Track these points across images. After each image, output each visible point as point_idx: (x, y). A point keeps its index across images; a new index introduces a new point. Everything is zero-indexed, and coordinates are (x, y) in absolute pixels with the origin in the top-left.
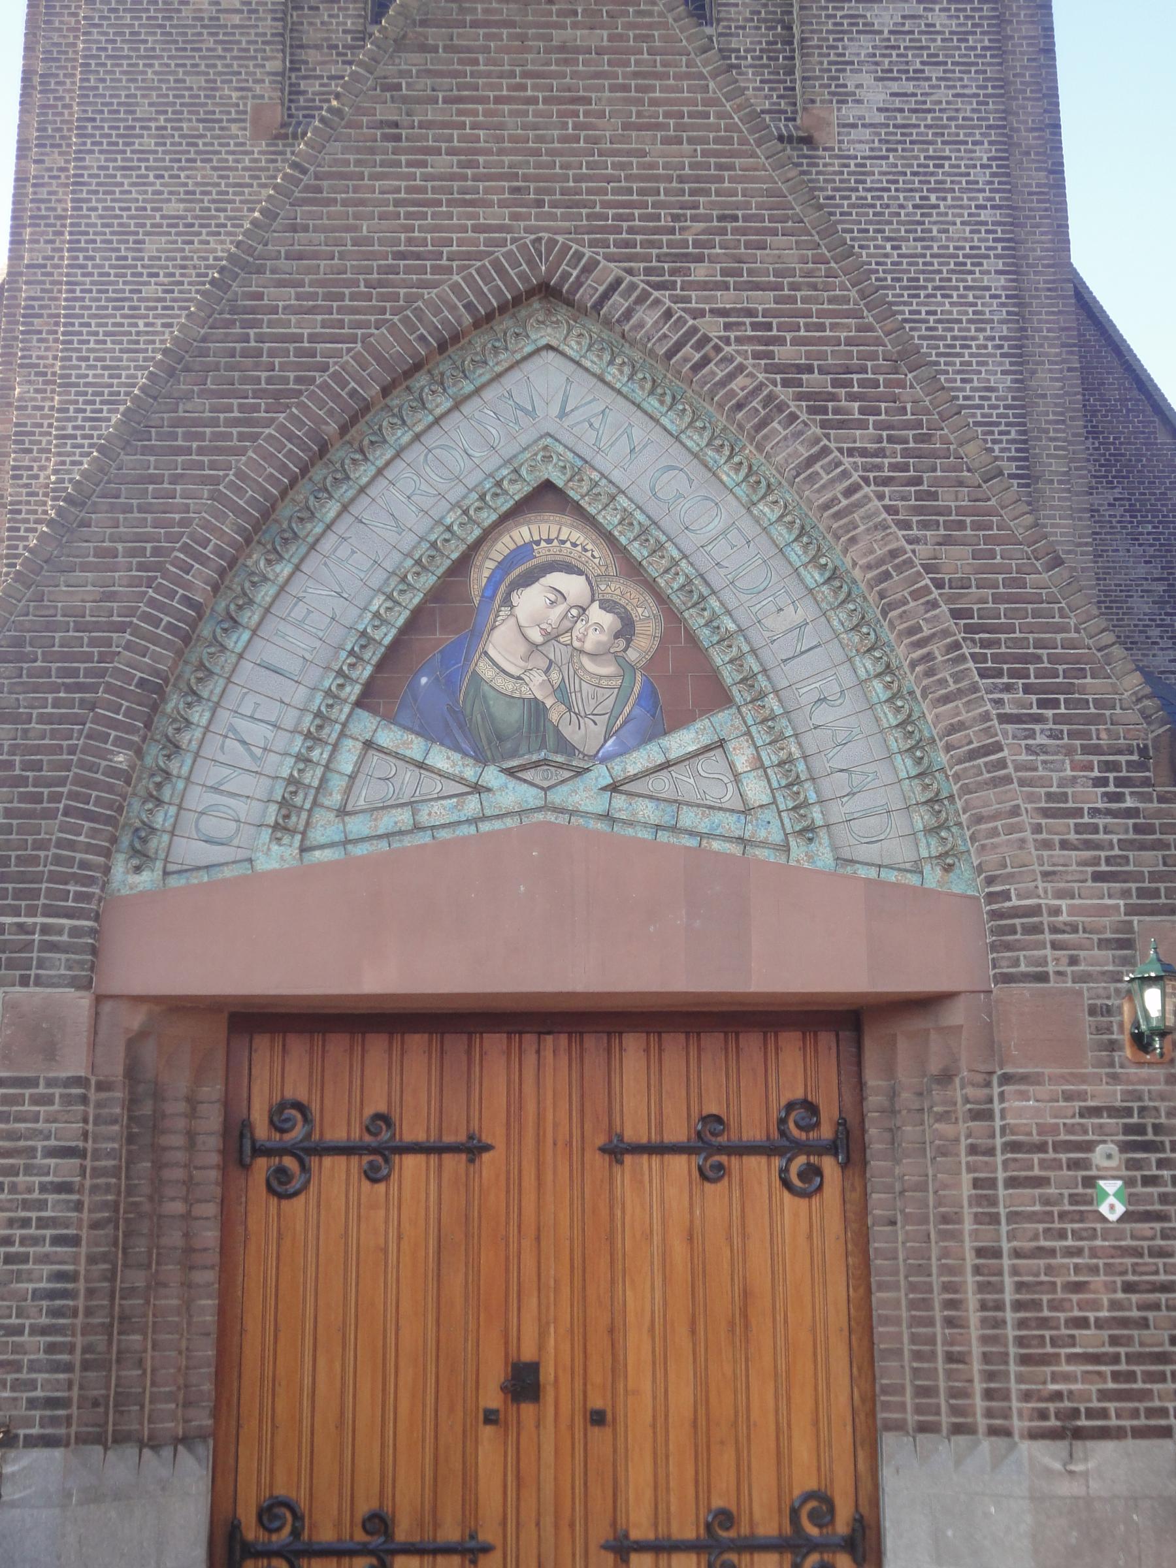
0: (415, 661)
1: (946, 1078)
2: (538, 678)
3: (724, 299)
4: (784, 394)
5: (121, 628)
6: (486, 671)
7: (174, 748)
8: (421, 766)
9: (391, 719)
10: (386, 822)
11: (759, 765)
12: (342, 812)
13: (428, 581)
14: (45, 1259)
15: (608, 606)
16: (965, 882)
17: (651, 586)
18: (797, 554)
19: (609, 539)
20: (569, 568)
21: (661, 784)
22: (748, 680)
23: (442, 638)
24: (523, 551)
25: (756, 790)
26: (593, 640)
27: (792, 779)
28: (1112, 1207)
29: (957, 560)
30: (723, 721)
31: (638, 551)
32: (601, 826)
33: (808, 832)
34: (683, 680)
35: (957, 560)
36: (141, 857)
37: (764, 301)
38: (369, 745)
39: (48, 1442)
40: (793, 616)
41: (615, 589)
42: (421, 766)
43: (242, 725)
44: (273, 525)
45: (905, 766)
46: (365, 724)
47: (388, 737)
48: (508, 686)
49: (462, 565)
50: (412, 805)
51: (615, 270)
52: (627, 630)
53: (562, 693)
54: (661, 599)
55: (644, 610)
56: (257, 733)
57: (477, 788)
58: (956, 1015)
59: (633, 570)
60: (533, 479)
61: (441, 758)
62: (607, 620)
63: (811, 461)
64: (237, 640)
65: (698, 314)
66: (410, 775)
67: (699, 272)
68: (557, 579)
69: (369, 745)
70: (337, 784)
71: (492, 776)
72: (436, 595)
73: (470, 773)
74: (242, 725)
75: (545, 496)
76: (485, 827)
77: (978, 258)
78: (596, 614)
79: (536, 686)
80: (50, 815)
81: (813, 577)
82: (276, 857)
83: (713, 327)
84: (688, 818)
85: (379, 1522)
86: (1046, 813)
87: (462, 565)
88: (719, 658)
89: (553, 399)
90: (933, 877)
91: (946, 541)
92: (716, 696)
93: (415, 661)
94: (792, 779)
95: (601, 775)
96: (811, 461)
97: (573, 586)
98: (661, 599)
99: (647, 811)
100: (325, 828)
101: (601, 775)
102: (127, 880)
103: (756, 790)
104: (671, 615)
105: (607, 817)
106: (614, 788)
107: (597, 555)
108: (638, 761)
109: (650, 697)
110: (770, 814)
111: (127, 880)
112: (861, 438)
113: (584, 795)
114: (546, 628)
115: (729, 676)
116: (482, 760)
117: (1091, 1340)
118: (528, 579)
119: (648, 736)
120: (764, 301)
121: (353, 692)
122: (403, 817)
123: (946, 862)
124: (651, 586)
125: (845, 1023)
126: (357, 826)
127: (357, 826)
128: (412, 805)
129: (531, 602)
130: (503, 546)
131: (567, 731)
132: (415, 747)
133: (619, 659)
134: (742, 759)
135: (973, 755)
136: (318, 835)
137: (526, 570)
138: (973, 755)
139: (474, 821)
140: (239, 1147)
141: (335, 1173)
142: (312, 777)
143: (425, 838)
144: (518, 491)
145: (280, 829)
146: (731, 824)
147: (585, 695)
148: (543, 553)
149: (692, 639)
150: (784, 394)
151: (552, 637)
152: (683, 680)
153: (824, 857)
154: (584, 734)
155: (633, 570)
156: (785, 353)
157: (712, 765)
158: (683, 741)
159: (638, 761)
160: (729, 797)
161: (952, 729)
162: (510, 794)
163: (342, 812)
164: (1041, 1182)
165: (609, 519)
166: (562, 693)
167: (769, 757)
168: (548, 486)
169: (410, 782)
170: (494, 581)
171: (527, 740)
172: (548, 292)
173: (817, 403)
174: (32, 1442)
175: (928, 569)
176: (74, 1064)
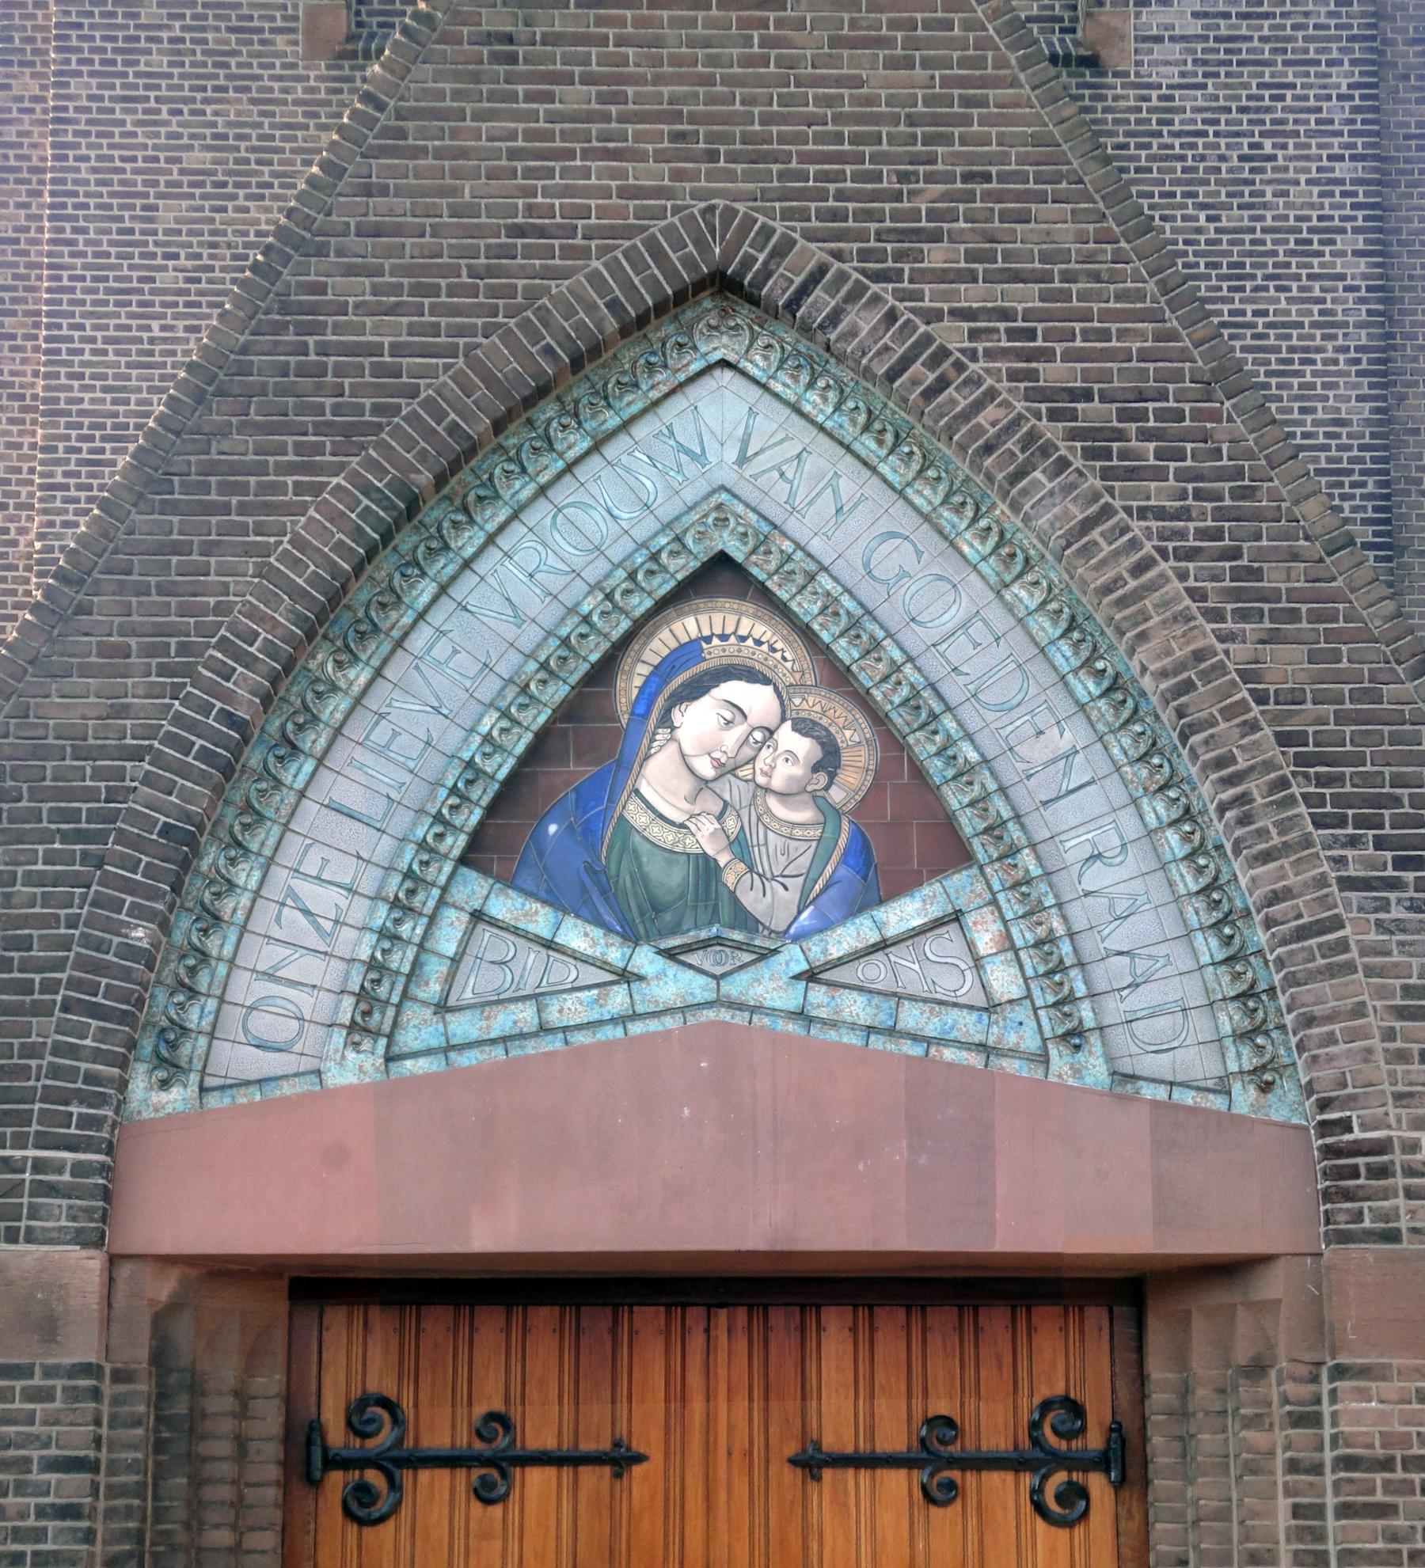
0: (541, 802)
1: (1257, 1369)
2: (706, 828)
3: (970, 296)
4: (1051, 431)
5: (137, 755)
6: (637, 816)
7: (212, 920)
8: (549, 945)
9: (508, 881)
10: (503, 1021)
11: (1008, 945)
13: (558, 692)
15: (803, 727)
16: (1287, 1107)
17: (863, 700)
18: (1064, 655)
19: (806, 634)
20: (751, 675)
21: (874, 971)
22: (994, 830)
23: (580, 771)
24: (689, 651)
25: (1004, 980)
27: (1055, 965)
29: (1287, 665)
30: (961, 885)
31: (845, 651)
32: (793, 1027)
33: (1074, 1038)
34: (907, 827)
35: (1287, 665)
36: (169, 1069)
37: (1025, 298)
42: (549, 945)
43: (303, 888)
44: (345, 614)
45: (1209, 947)
46: (473, 888)
47: (504, 906)
48: (664, 836)
50: (537, 998)
51: (817, 252)
52: (829, 760)
53: (740, 847)
54: (878, 718)
55: (853, 733)
56: (325, 900)
57: (625, 976)
58: (1272, 1285)
60: (700, 552)
61: (576, 935)
62: (803, 747)
63: (1087, 525)
64: (296, 773)
66: (532, 958)
67: (936, 256)
68: (733, 690)
70: (436, 969)
71: (645, 960)
72: (568, 712)
73: (616, 955)
74: (303, 888)
75: (720, 575)
76: (636, 1028)
78: (787, 737)
79: (706, 837)
81: (1086, 687)
82: (352, 1068)
83: (953, 335)
84: (912, 1017)
86: (1402, 1013)
88: (954, 799)
89: (728, 434)
90: (1244, 1098)
91: (1273, 638)
92: (954, 853)
93: (541, 802)
94: (1055, 965)
95: (793, 959)
96: (1087, 525)
97: (758, 700)
98: (878, 718)
99: (855, 1007)
101: (793, 959)
102: (149, 1098)
103: (1004, 980)
104: (890, 740)
105: (800, 1015)
106: (811, 976)
109: (861, 854)
110: (1022, 1013)
111: (149, 1098)
112: (1157, 493)
113: (770, 986)
114: (723, 759)
115: (969, 823)
116: (632, 937)
118: (696, 690)
120: (1025, 298)
121: (456, 844)
122: (525, 1015)
123: (1264, 1078)
124: (863, 700)
125: (1124, 1294)
126: (463, 1026)
127: (463, 1026)
128: (537, 998)
129: (699, 722)
131: (751, 900)
132: (541, 919)
133: (818, 799)
134: (985, 939)
135: (1301, 934)
136: (409, 1039)
138: (1301, 934)
139: (621, 1020)
140: (306, 1456)
141: (435, 1495)
143: (554, 1043)
144: (681, 567)
145: (357, 1029)
146: (968, 1025)
147: (771, 849)
148: (716, 653)
149: (919, 772)
150: (1051, 431)
151: (727, 770)
152: (907, 827)
153: (1095, 1071)
154: (771, 902)
155: (838, 677)
156: (1054, 372)
157: (945, 945)
158: (904, 913)
160: (967, 989)
161: (1274, 898)
162: (670, 984)
163: (443, 1007)
164: (1384, 1511)
165: (806, 607)
166: (740, 847)
167: (1022, 935)
168: (722, 560)
169: (536, 968)
170: (648, 694)
171: (693, 910)
172: (726, 287)
173: (1097, 444)
175: (1247, 676)
176: (82, 1348)
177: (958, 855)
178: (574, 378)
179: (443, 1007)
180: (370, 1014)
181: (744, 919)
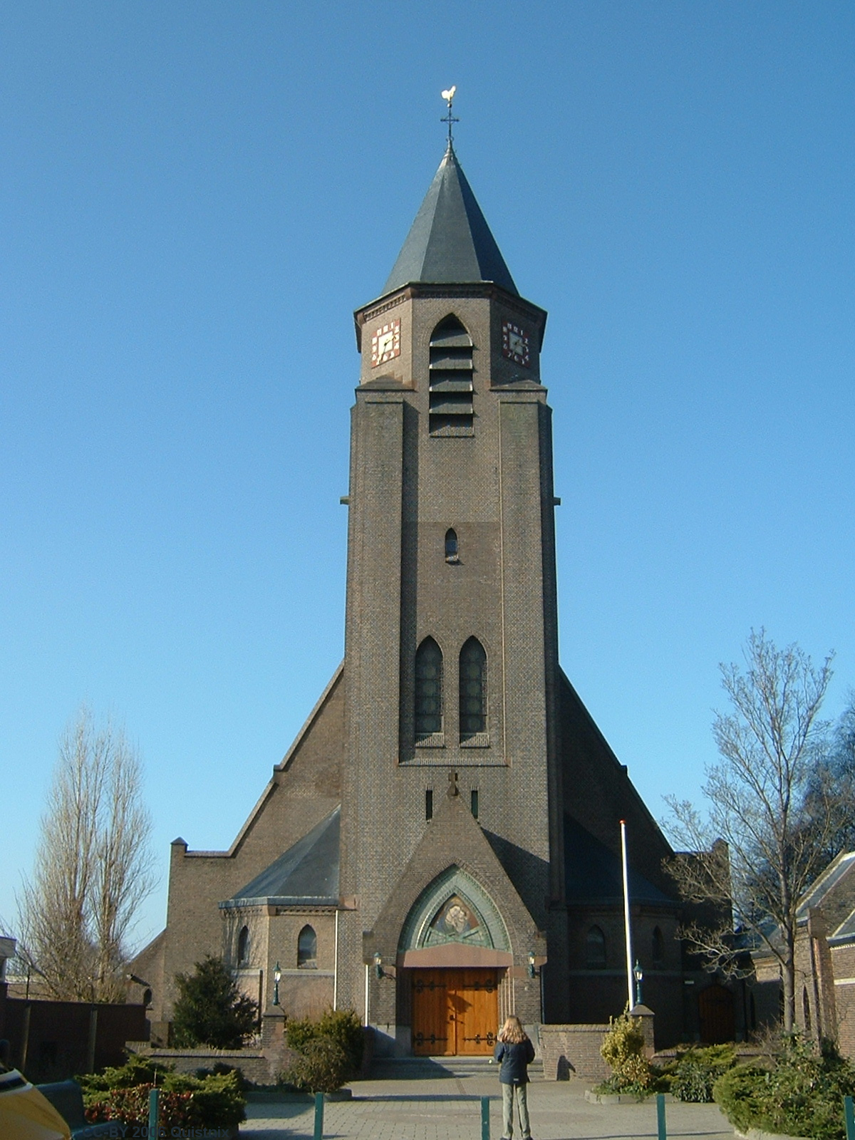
3: (479, 866)
11: (483, 935)
13: (438, 908)
15: (463, 911)
20: (457, 905)
25: (483, 938)
26: (460, 916)
37: (485, 866)
40: (489, 913)
50: (437, 940)
52: (465, 914)
60: (452, 893)
61: (440, 934)
64: (413, 917)
67: (476, 862)
68: (456, 907)
77: (540, 792)
78: (461, 912)
79: (453, 923)
85: (433, 1036)
94: (489, 937)
97: (458, 908)
101: (462, 936)
103: (483, 938)
107: (461, 904)
109: (468, 925)
114: (454, 914)
117: (523, 1012)
120: (485, 866)
129: (452, 910)
131: (457, 930)
134: (481, 934)
140: (413, 986)
141: (426, 990)
143: (438, 946)
144: (450, 895)
147: (459, 924)
151: (455, 916)
156: (488, 874)
158: (473, 931)
159: (467, 934)
160: (479, 939)
166: (456, 924)
167: (485, 934)
171: (451, 931)
173: (492, 882)
177: (478, 925)
181: (457, 932)
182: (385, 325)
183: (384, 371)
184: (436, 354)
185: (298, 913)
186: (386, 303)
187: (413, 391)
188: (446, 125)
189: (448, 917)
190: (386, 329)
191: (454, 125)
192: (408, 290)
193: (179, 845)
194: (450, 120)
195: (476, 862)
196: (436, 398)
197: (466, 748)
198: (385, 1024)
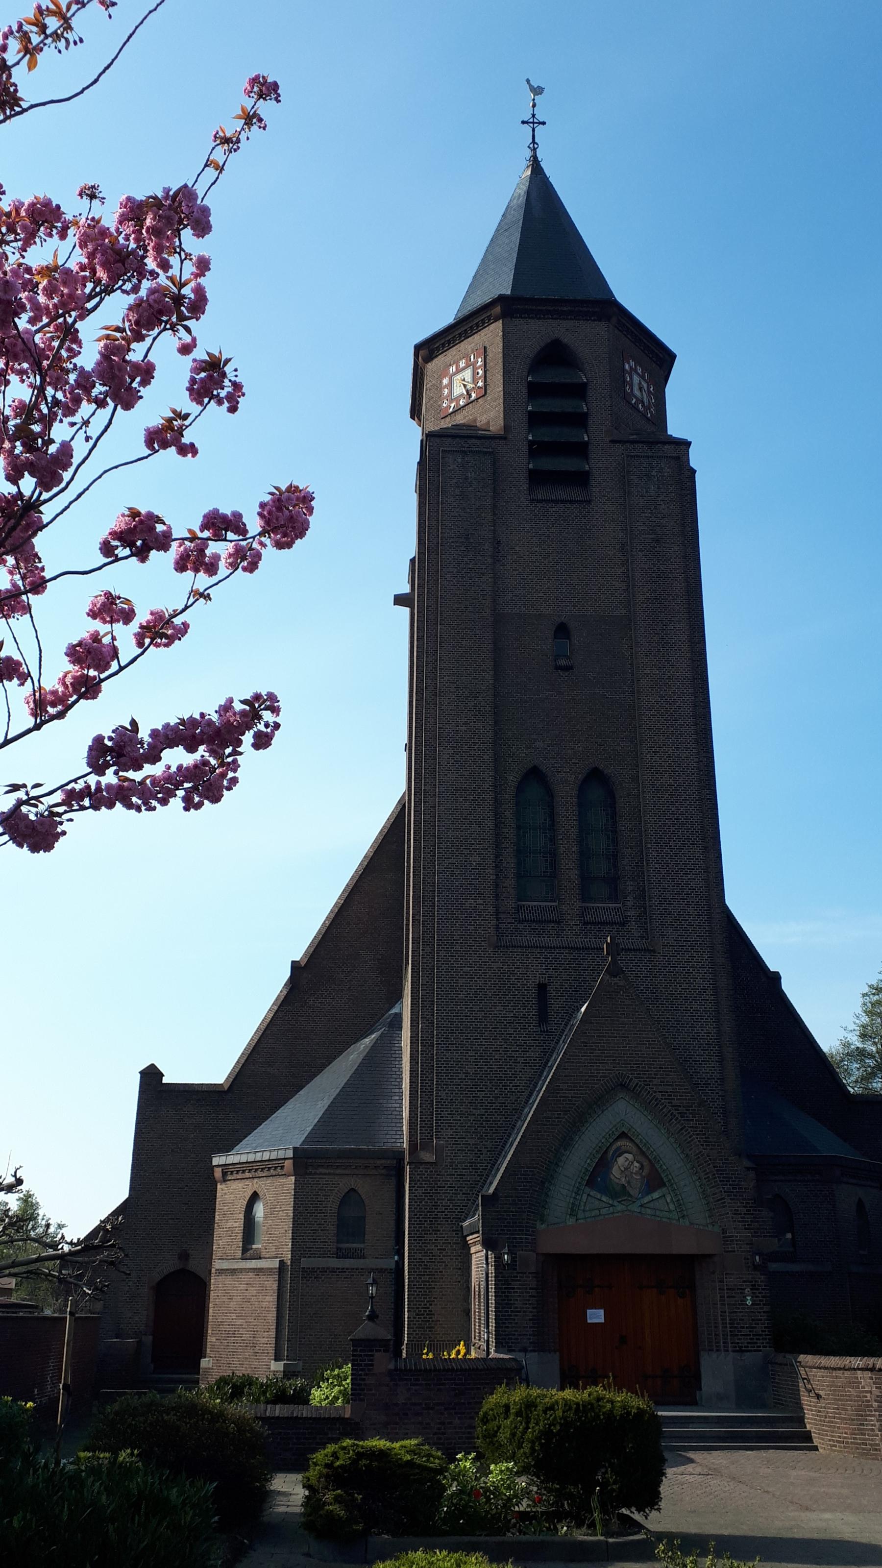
0: (597, 1176)
1: (713, 1273)
2: (623, 1180)
3: (661, 1089)
4: (675, 1112)
5: (535, 1168)
6: (613, 1178)
7: (547, 1195)
8: (600, 1200)
12: (584, 1211)
14: (531, 1312)
17: (647, 1157)
18: (679, 1151)
19: (637, 1145)
21: (651, 1205)
22: (669, 1181)
24: (619, 1148)
25: (672, 1207)
28: (749, 1303)
30: (664, 1189)
31: (644, 1149)
32: (639, 1215)
34: (655, 1180)
36: (543, 1221)
37: (670, 1089)
38: (589, 1195)
39: (534, 1351)
41: (640, 1158)
42: (600, 1200)
43: (561, 1190)
44: (566, 1142)
46: (587, 1190)
48: (617, 1181)
49: (606, 1152)
50: (599, 1209)
52: (642, 1167)
54: (650, 1161)
55: (646, 1163)
57: (612, 1206)
59: (643, 1153)
61: (604, 1199)
63: (682, 1129)
65: (655, 1092)
67: (655, 1081)
68: (626, 1155)
69: (589, 1195)
70: (582, 1204)
72: (601, 1159)
73: (611, 1202)
74: (561, 1190)
75: (623, 1135)
76: (616, 1215)
78: (636, 1164)
79: (623, 1181)
80: (524, 1212)
81: (682, 1156)
82: (571, 1221)
83: (659, 1096)
84: (658, 1213)
86: (735, 1214)
87: (606, 1152)
89: (623, 1111)
90: (710, 1227)
91: (711, 1149)
92: (662, 1184)
93: (597, 1176)
95: (638, 1203)
96: (682, 1129)
98: (650, 1161)
99: (649, 1211)
100: (581, 1215)
102: (541, 1227)
103: (672, 1207)
106: (641, 1206)
107: (634, 1149)
108: (646, 1200)
110: (675, 1213)
111: (541, 1227)
113: (635, 1208)
114: (625, 1166)
115: (665, 1180)
116: (612, 1198)
117: (745, 1331)
118: (620, 1155)
119: (648, 1193)
120: (670, 1089)
122: (597, 1212)
124: (647, 1157)
125: (691, 1261)
126: (588, 1214)
127: (588, 1214)
128: (599, 1209)
129: (621, 1160)
130: (614, 1147)
131: (632, 1193)
132: (599, 1196)
133: (641, 1174)
135: (719, 1200)
136: (579, 1216)
137: (619, 1153)
138: (719, 1200)
139: (613, 1213)
142: (577, 1203)
143: (602, 1217)
144: (617, 1134)
149: (657, 1170)
150: (675, 1112)
151: (626, 1169)
152: (655, 1180)
153: (687, 1223)
155: (643, 1153)
156: (675, 1102)
158: (656, 1195)
160: (666, 1208)
161: (714, 1194)
162: (620, 1207)
164: (734, 1297)
165: (638, 1141)
166: (629, 1182)
168: (623, 1132)
170: (613, 1155)
172: (623, 1086)
173: (682, 1115)
174: (531, 1351)
175: (708, 1156)
176: (533, 1269)
177: (664, 1185)
178: (599, 1101)
179: (584, 1211)
180: (573, 1213)
181: (630, 1195)
182: (461, 359)
183: (460, 419)
184: (535, 391)
185: (338, 1171)
186: (463, 329)
187: (505, 438)
188: (528, 129)
189: (615, 1172)
190: (462, 364)
191: (539, 129)
192: (498, 310)
193: (151, 1077)
194: (533, 123)
195: (655, 1081)
196: (536, 449)
197: (592, 923)
198: (520, 1351)
